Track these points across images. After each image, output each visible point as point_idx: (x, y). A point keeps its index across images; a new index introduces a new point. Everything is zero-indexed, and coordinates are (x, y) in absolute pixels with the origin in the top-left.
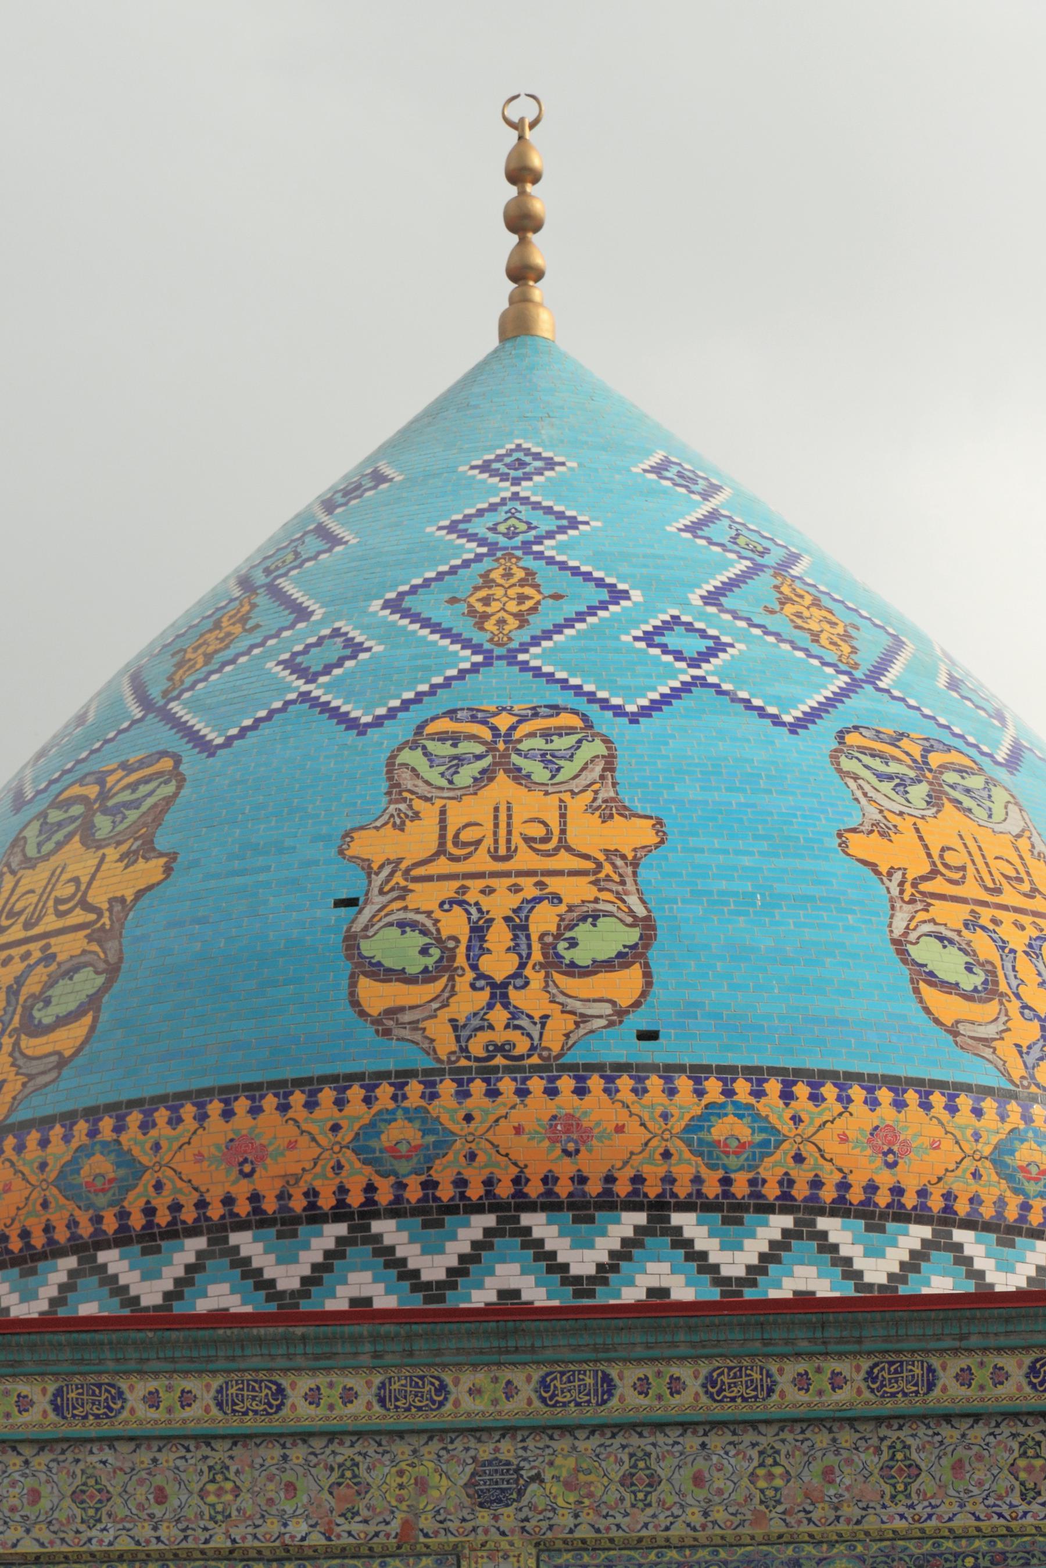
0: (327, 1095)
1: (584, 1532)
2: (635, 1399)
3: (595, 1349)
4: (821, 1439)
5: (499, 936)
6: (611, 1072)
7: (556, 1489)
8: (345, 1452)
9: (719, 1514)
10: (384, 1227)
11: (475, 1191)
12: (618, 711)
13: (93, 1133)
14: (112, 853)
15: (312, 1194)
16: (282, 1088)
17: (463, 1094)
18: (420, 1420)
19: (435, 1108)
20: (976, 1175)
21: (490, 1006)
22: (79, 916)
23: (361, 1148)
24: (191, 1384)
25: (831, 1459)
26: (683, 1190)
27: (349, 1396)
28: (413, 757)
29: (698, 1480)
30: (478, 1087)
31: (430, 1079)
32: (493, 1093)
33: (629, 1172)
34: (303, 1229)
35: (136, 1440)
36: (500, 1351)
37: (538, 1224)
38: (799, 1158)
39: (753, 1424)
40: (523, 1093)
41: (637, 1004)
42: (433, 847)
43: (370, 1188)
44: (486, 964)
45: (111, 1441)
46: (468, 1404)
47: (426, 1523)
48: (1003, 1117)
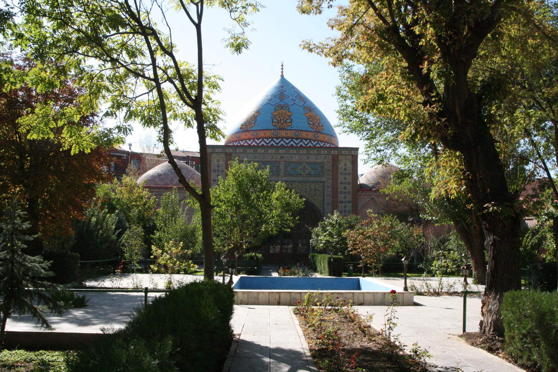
5: (282, 120)
6: (289, 130)
10: (274, 139)
16: (268, 130)
37: (284, 139)
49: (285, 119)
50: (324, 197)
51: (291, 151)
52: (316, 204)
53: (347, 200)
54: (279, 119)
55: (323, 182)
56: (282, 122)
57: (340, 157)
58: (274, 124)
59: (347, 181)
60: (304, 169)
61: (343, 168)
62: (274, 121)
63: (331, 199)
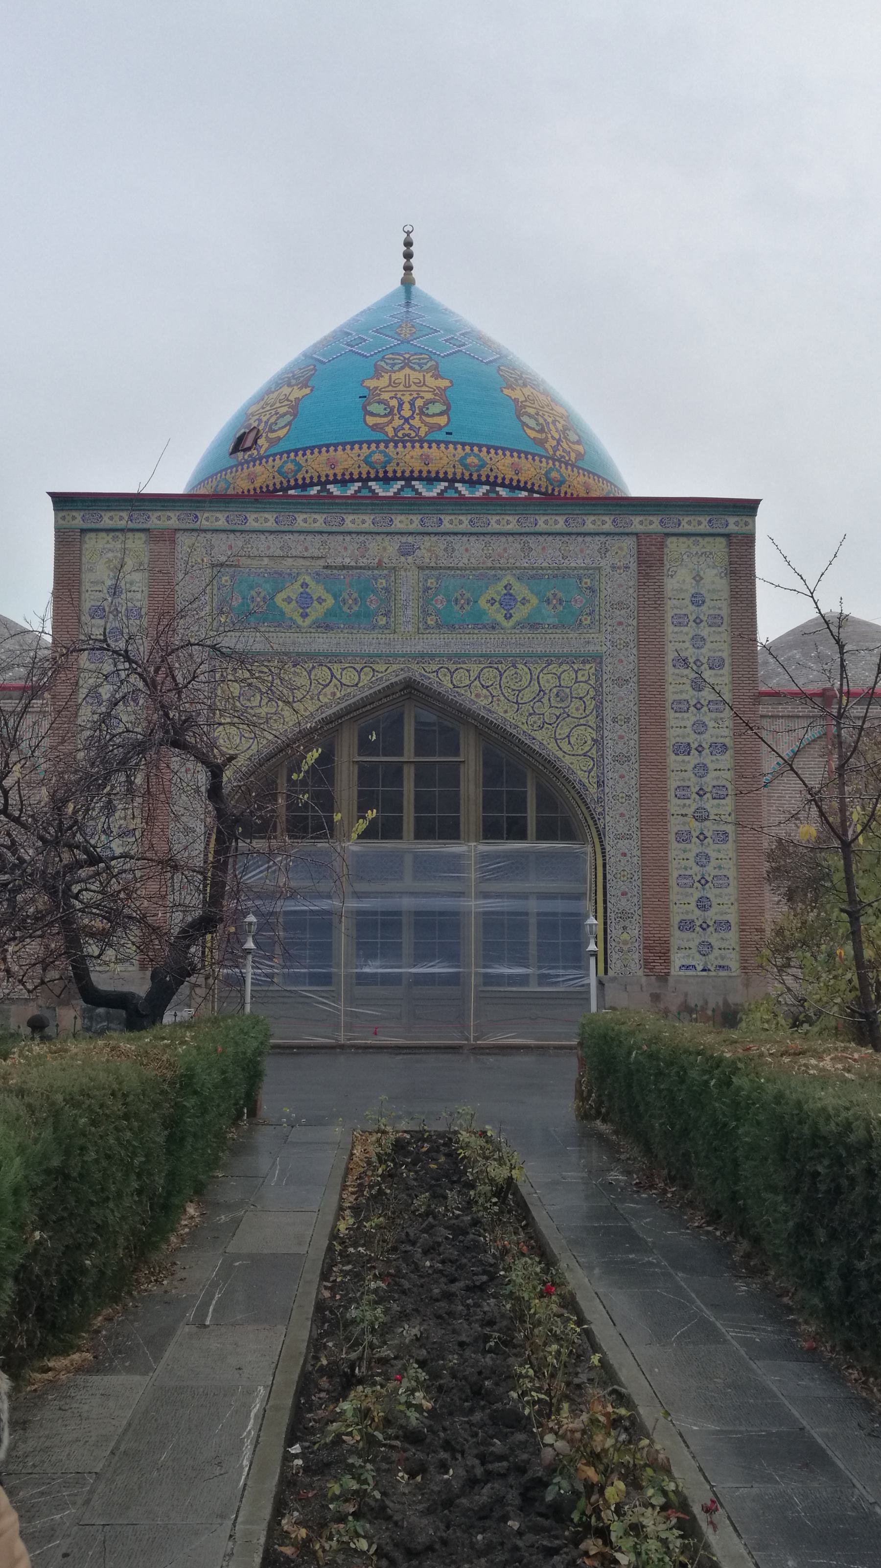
0: (357, 446)
1: (433, 564)
2: (448, 525)
3: (437, 510)
4: (503, 539)
5: (406, 406)
6: (438, 443)
7: (424, 551)
8: (362, 538)
9: (473, 560)
11: (399, 475)
12: (439, 355)
13: (288, 457)
14: (295, 388)
15: (351, 474)
16: (344, 445)
17: (396, 447)
18: (385, 530)
19: (387, 450)
20: (540, 479)
21: (404, 424)
22: (286, 403)
23: (366, 461)
24: (317, 516)
25: (506, 545)
26: (458, 477)
27: (363, 522)
28: (382, 364)
29: (467, 550)
30: (400, 445)
31: (387, 443)
32: (405, 447)
33: (444, 470)
34: (349, 484)
35: (300, 532)
36: (409, 510)
38: (491, 470)
39: (484, 534)
40: (413, 447)
41: (445, 426)
42: (387, 382)
43: (368, 473)
44: (402, 413)
45: (292, 532)
46: (399, 525)
47: (385, 560)
48: (548, 463)
49: (419, 403)
50: (599, 728)
51: (446, 519)
52: (567, 760)
53: (707, 738)
54: (394, 403)
55: (597, 659)
56: (406, 413)
57: (672, 544)
58: (371, 420)
59: (705, 652)
60: (508, 601)
61: (688, 596)
62: (371, 408)
63: (636, 737)
